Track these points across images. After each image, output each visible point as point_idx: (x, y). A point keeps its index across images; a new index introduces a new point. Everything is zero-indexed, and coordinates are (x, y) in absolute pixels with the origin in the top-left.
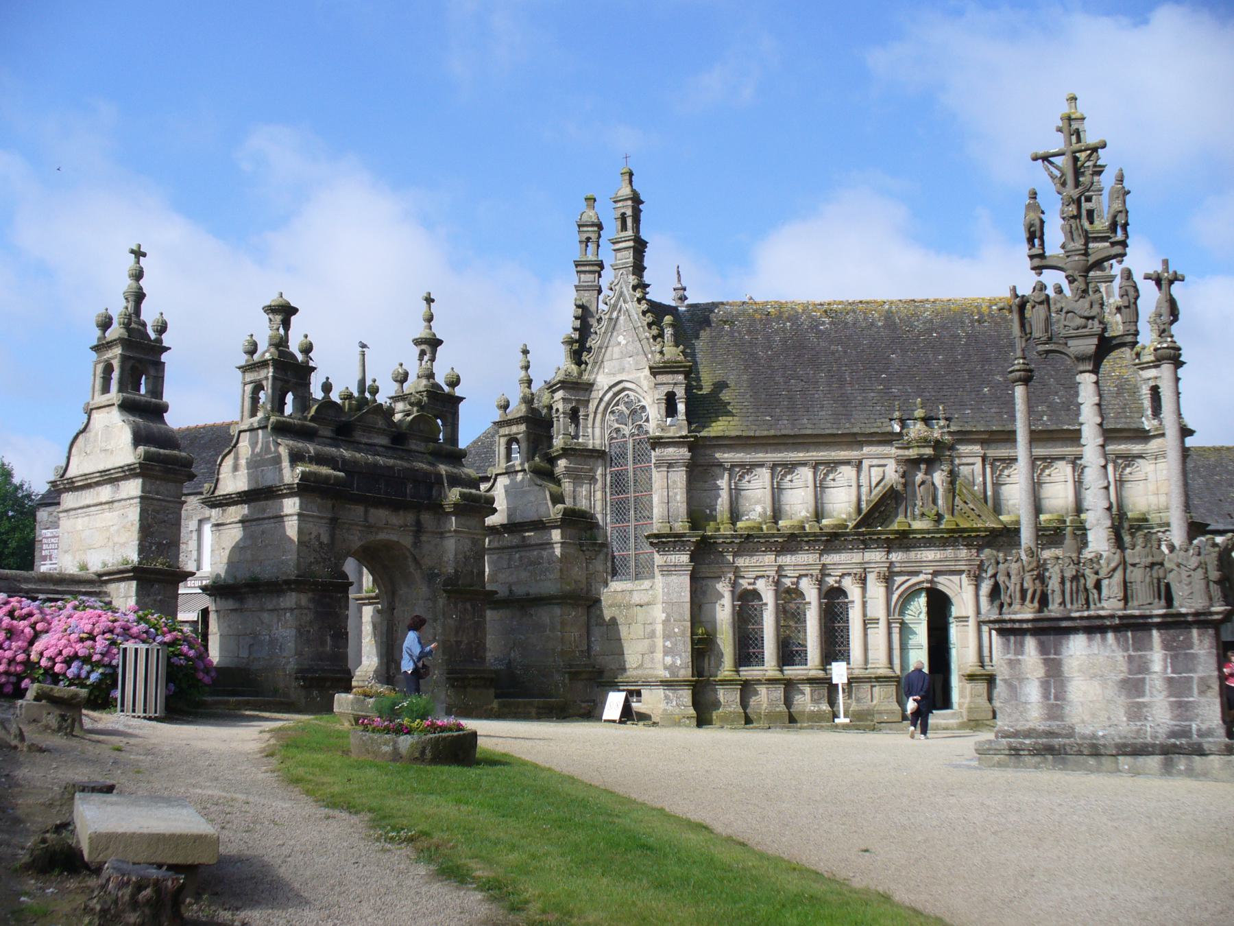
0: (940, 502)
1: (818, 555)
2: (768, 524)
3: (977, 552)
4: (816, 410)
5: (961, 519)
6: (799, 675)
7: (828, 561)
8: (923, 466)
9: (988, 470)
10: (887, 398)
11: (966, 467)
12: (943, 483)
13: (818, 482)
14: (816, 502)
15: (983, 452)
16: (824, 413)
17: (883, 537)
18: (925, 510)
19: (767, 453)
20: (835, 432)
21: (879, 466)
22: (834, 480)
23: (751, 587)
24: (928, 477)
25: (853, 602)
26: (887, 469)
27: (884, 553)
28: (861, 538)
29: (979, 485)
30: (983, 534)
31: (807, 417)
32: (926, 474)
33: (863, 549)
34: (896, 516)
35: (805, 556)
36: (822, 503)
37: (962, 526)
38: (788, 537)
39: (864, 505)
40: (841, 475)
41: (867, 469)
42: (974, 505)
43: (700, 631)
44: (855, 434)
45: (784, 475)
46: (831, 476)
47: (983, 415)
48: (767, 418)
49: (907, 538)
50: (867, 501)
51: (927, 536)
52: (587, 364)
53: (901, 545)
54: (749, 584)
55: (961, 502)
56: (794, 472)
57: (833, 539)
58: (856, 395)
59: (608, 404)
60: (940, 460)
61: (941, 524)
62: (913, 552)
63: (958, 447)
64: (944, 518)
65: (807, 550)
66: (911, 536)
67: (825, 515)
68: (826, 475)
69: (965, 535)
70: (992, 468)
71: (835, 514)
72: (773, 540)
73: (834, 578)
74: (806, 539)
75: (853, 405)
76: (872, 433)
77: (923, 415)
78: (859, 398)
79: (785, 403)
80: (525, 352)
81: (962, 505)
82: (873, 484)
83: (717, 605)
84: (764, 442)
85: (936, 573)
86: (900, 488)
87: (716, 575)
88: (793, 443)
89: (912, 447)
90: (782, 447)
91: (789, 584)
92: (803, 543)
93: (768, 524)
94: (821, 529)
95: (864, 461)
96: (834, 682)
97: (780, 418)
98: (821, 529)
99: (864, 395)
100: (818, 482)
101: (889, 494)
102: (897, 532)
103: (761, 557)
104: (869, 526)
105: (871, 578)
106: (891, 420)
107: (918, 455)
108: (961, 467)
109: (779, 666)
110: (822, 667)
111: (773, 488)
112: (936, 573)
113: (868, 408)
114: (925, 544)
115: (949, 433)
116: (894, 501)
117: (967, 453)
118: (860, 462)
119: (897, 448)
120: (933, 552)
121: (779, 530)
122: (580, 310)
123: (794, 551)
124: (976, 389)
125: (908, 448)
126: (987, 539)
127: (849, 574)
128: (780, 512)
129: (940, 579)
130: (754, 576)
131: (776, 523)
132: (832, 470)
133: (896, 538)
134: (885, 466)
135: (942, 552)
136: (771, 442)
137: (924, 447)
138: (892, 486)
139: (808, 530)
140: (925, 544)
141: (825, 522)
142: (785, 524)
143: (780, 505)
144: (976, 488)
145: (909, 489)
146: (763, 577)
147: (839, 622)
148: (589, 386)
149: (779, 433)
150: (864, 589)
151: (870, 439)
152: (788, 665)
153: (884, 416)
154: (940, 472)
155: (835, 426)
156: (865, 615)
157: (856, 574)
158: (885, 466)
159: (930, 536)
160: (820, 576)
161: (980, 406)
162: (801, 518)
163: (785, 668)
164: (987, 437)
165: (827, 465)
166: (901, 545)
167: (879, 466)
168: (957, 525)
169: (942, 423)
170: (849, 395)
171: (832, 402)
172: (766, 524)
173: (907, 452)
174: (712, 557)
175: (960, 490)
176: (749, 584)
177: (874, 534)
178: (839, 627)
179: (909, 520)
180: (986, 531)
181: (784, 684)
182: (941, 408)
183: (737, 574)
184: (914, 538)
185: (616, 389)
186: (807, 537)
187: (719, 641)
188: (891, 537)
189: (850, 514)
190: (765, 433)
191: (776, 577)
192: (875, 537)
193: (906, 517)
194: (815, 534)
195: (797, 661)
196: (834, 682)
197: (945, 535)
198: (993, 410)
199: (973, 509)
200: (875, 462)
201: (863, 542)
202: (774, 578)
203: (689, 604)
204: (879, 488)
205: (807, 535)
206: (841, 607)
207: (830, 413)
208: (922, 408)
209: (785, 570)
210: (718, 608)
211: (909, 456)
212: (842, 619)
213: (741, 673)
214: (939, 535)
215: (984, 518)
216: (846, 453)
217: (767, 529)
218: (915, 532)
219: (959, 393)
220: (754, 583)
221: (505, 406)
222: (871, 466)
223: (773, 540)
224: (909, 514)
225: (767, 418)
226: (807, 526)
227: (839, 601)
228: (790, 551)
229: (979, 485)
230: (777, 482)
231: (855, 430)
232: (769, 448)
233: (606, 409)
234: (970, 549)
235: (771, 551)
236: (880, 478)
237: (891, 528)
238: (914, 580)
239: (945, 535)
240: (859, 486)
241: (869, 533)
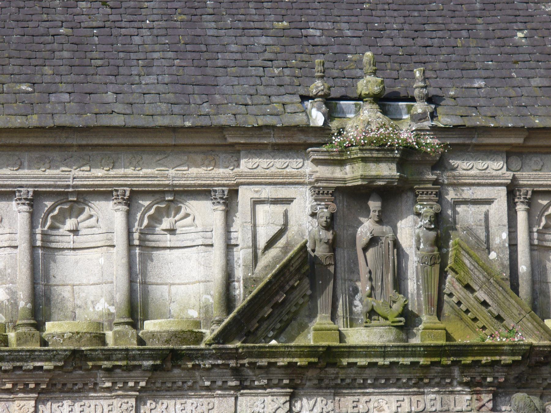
0: (412, 285)
1: (133, 402)
2: (21, 330)
3: (494, 399)
4: (135, 71)
5: (460, 324)
8: (374, 205)
9: (522, 216)
10: (296, 49)
11: (473, 209)
12: (418, 241)
13: (136, 235)
14: (132, 281)
15: (510, 174)
16: (152, 79)
17: (282, 362)
18: (378, 303)
19: (21, 167)
20: (178, 122)
21: (276, 201)
22: (172, 231)
24: (386, 229)
26: (293, 208)
27: (283, 399)
28: (232, 363)
29: (499, 249)
30: (507, 359)
31: (116, 88)
32: (380, 222)
33: (237, 388)
34: (312, 315)
35: (105, 403)
36: (144, 283)
37: (459, 341)
38: (66, 359)
39: (239, 290)
40: (189, 220)
41: (249, 208)
42: (488, 294)
44: (222, 129)
45: (61, 218)
46: (166, 223)
47: (512, 93)
48: (24, 87)
49: (334, 365)
50: (246, 280)
51: (380, 361)
53: (321, 380)
55: (458, 286)
56: (82, 211)
57: (169, 365)
58: (226, 40)
60: (412, 190)
61: (414, 335)
62: (350, 399)
63: (454, 162)
64: (420, 322)
65: (108, 389)
66: (345, 362)
67: (152, 308)
68: (155, 219)
69: (468, 360)
70: (529, 212)
71: (174, 308)
72: (31, 365)
74: (106, 364)
75: (219, 63)
76: (260, 128)
77: (376, 89)
78: (233, 48)
79: (66, 54)
81: (460, 292)
82: (262, 243)
84: (15, 141)
86: (321, 251)
88: (80, 146)
89: (352, 161)
90: (55, 155)
92: (100, 374)
93: (21, 330)
94: (141, 341)
95: (242, 190)
97: (53, 88)
98: (141, 341)
99: (245, 40)
100: (136, 235)
101: (296, 264)
102: (312, 351)
104: (249, 336)
106: (304, 98)
107: (363, 178)
108: (460, 209)
111: (33, 247)
113: (253, 71)
114: (376, 379)
115: (434, 129)
116: (306, 282)
117: (474, 177)
118: (234, 193)
119: (317, 162)
120: (393, 398)
121: (44, 343)
123: (79, 391)
124: (498, 33)
125: (341, 163)
126: (515, 372)
128: (48, 299)
131: (39, 326)
132: (168, 208)
133: (311, 365)
134: (288, 201)
135: (415, 398)
136: (31, 141)
137: (378, 160)
138: (304, 247)
139: (111, 343)
140: (376, 379)
141: (150, 326)
142: (59, 331)
143: (48, 286)
144: (493, 255)
145: (342, 254)
149: (49, 122)
151: (256, 141)
153: (290, 89)
154: (411, 218)
155: (176, 109)
158: (288, 201)
159: (387, 361)
161: (504, 73)
162: (95, 317)
164: (520, 141)
165: (157, 196)
166: (321, 380)
167: (276, 201)
168: (449, 337)
169: (419, 107)
170: (211, 41)
171: (170, 55)
172: (15, 327)
173: (337, 173)
175: (457, 260)
177: (262, 355)
179: (340, 324)
180: (513, 353)
182: (418, 75)
184: (351, 365)
186: (108, 359)
188: (301, 362)
189: (206, 309)
190: (18, 122)
192: (263, 362)
193: (333, 317)
194: (126, 354)
197: (422, 361)
198: (536, 82)
199: (485, 304)
200: (267, 192)
201: (237, 372)
204: (274, 252)
205: (109, 354)
207: (167, 79)
208: (374, 73)
211: (344, 180)
214: (407, 361)
215: (510, 323)
216: (202, 171)
217: (19, 339)
218: (353, 351)
219: (459, 43)
222: (256, 202)
223: (31, 365)
224: (340, 311)
225: (24, 87)
226: (109, 335)
228: (71, 391)
229: (499, 249)
230: (44, 234)
231: (224, 120)
232: (26, 156)
234: (478, 393)
235: (26, 390)
236: (278, 228)
237: (300, 341)
239: (422, 361)
240: (229, 247)
241: (250, 354)
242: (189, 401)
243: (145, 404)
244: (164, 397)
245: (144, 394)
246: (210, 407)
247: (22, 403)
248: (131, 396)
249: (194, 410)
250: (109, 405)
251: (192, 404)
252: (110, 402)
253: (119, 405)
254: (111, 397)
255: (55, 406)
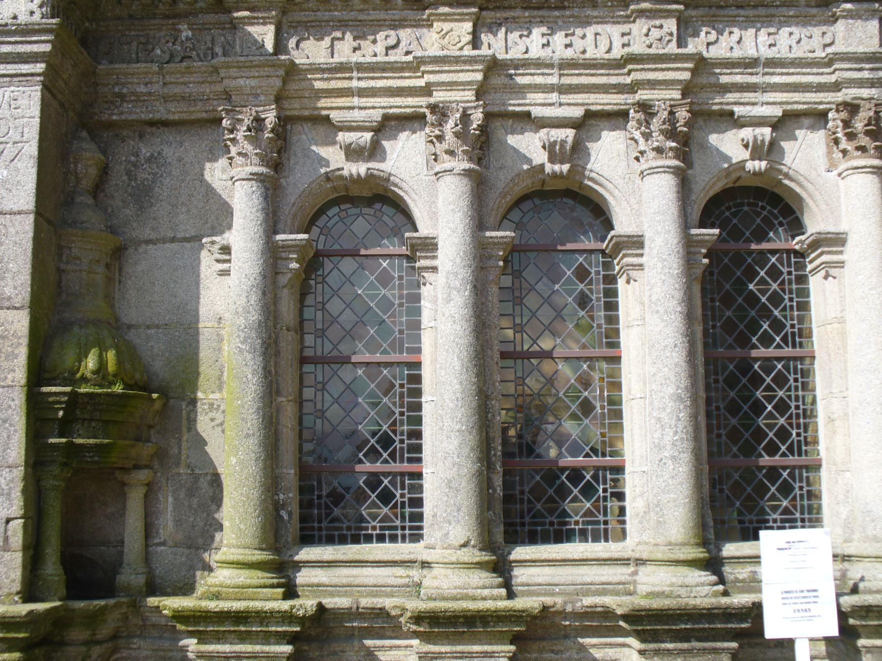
1: (671, 25)
6: (587, 589)
7: (714, 53)
23: (360, 169)
25: (837, 240)
43: (91, 363)
54: (353, 153)
73: (747, 133)
83: (204, 254)
87: (198, 112)
91: (540, 157)
96: (772, 630)
103: (405, 34)
109: (487, 545)
110: (698, 553)
127: (819, 117)
130: (376, 115)
146: (413, 120)
147: (767, 341)
152: (533, 539)
157: (852, 108)
160: (683, 114)
163: (520, 552)
174: (186, 33)
176: (353, 153)
178: (768, 364)
181: (515, 639)
183: (294, 108)
187: (204, 425)
191: (477, 117)
195: (576, 521)
196: (772, 630)
202: (465, 117)
203: (27, 224)
206: (774, 273)
209: (522, 90)
210: (208, 263)
212: (777, 326)
213: (303, 577)
220: (374, 151)
227: (765, 246)
242: (785, 31)
243: (696, 34)
244: (732, 22)
245: (694, 13)
246: (828, 40)
247: (447, 26)
248: (668, 14)
249: (794, 45)
250: (623, 35)
251: (791, 34)
252: (625, 28)
253: (645, 31)
254: (628, 19)
255: (514, 36)
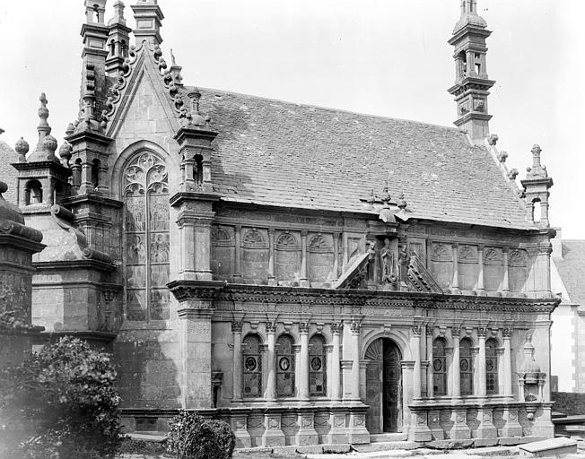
52: (106, 120)
59: (127, 160)
80: (44, 101)
85: (393, 327)
105: (347, 328)
112: (393, 327)
122: (91, 73)
129: (395, 331)
148: (107, 143)
150: (341, 336)
156: (341, 358)
158: (359, 239)
185: (135, 148)
200: (352, 235)
205: (302, 290)
221: (23, 149)
222: (350, 238)
233: (124, 165)
238: (377, 331)
